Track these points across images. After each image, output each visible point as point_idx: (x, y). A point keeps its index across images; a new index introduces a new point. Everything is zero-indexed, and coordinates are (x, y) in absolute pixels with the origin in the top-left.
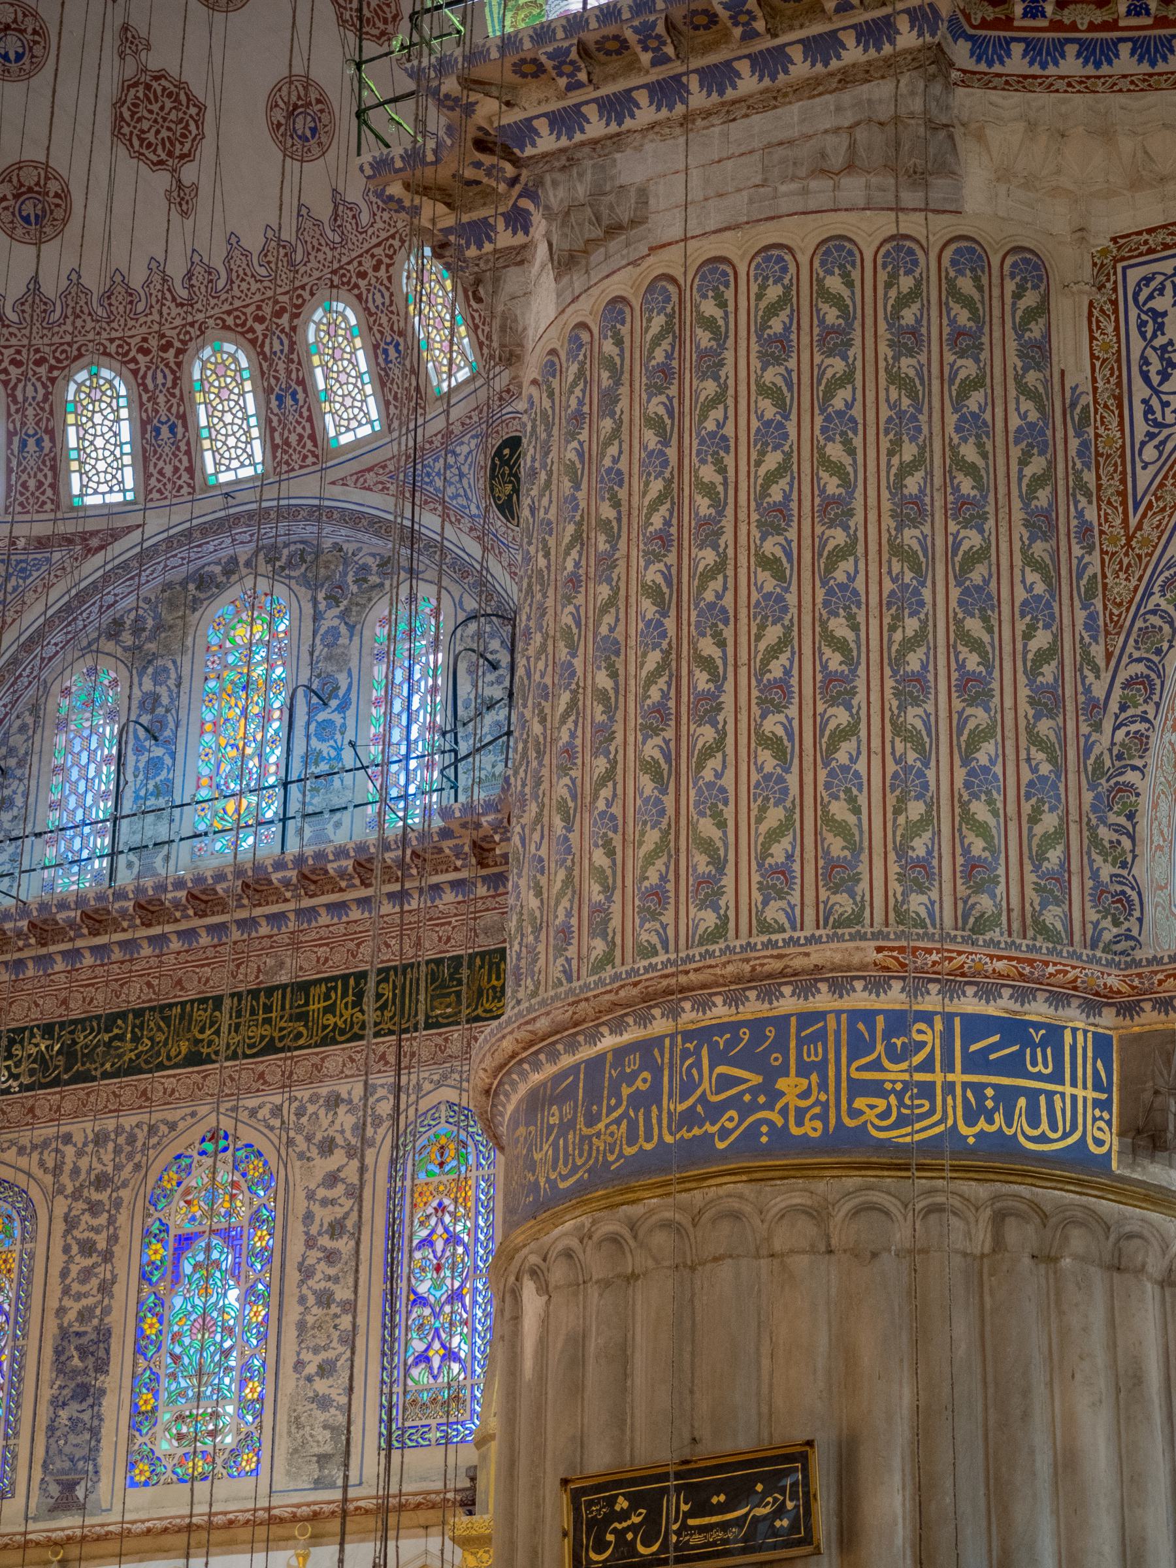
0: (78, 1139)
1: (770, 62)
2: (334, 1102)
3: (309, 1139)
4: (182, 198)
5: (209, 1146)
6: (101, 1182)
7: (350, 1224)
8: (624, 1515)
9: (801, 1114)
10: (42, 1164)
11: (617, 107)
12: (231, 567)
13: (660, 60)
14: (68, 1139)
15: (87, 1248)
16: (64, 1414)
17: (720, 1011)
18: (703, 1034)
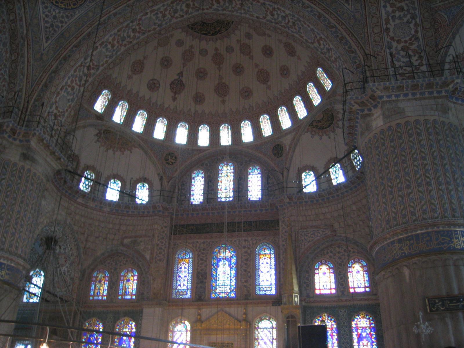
0: (200, 243)
1: (423, 94)
2: (245, 240)
3: (241, 246)
4: (224, 102)
5: (223, 246)
6: (204, 249)
7: (249, 259)
8: (438, 303)
9: (457, 245)
10: (193, 246)
11: (397, 96)
12: (223, 158)
13: (407, 90)
14: (198, 242)
15: (202, 260)
16: (199, 286)
17: (441, 228)
18: (438, 232)
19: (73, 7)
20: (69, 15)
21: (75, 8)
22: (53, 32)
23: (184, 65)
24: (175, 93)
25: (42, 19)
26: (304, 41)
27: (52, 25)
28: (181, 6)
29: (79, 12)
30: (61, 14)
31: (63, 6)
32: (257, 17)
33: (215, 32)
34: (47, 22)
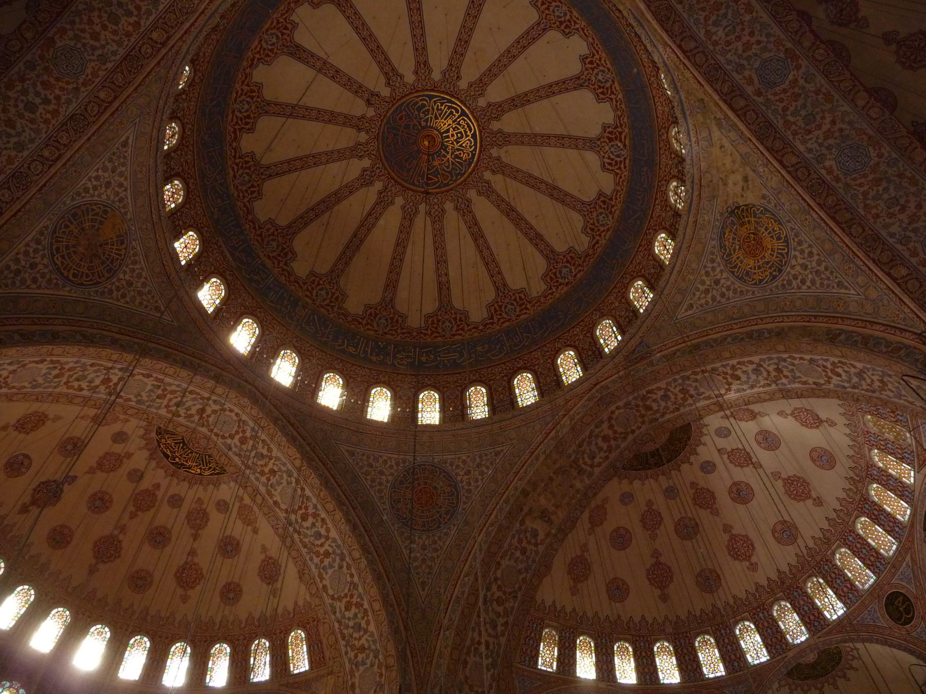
19: (71, 277)
20: (55, 281)
21: (70, 280)
22: (9, 282)
23: (91, 471)
24: (34, 502)
25: (16, 251)
26: (321, 586)
27: (18, 272)
28: (195, 405)
29: (71, 290)
30: (46, 271)
31: (59, 263)
32: (275, 503)
33: (182, 464)
34: (17, 261)
